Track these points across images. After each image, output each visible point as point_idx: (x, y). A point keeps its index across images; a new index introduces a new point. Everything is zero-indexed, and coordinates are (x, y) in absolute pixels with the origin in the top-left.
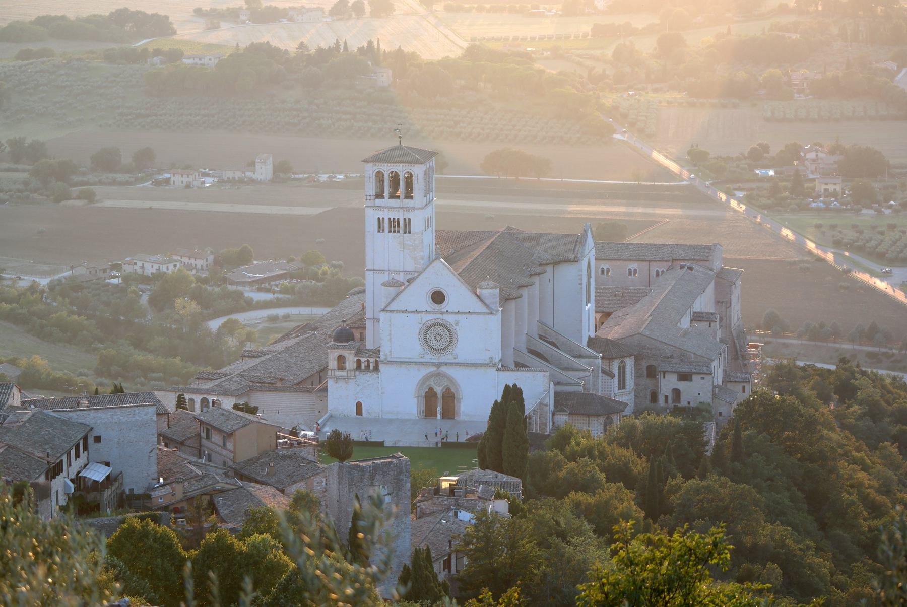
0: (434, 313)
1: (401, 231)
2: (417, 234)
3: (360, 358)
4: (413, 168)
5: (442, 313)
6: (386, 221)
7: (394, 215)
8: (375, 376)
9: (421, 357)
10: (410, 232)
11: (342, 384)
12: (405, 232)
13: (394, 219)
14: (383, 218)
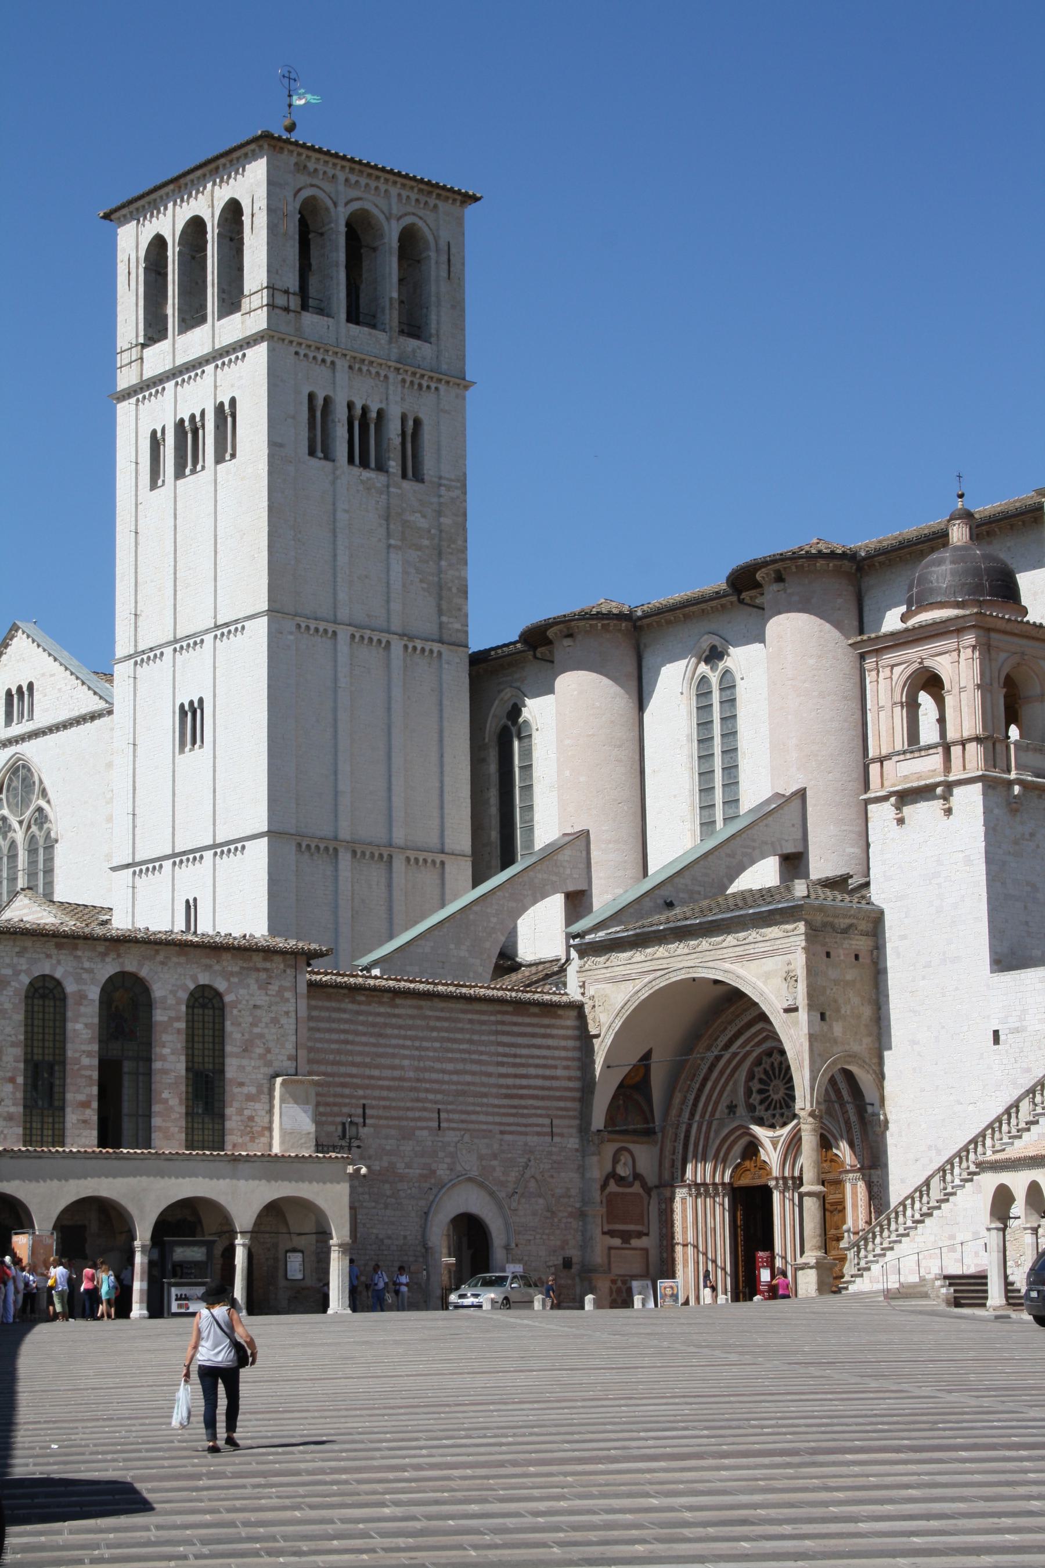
2: (449, 488)
6: (341, 414)
10: (418, 477)
12: (404, 476)
13: (365, 410)
14: (327, 400)
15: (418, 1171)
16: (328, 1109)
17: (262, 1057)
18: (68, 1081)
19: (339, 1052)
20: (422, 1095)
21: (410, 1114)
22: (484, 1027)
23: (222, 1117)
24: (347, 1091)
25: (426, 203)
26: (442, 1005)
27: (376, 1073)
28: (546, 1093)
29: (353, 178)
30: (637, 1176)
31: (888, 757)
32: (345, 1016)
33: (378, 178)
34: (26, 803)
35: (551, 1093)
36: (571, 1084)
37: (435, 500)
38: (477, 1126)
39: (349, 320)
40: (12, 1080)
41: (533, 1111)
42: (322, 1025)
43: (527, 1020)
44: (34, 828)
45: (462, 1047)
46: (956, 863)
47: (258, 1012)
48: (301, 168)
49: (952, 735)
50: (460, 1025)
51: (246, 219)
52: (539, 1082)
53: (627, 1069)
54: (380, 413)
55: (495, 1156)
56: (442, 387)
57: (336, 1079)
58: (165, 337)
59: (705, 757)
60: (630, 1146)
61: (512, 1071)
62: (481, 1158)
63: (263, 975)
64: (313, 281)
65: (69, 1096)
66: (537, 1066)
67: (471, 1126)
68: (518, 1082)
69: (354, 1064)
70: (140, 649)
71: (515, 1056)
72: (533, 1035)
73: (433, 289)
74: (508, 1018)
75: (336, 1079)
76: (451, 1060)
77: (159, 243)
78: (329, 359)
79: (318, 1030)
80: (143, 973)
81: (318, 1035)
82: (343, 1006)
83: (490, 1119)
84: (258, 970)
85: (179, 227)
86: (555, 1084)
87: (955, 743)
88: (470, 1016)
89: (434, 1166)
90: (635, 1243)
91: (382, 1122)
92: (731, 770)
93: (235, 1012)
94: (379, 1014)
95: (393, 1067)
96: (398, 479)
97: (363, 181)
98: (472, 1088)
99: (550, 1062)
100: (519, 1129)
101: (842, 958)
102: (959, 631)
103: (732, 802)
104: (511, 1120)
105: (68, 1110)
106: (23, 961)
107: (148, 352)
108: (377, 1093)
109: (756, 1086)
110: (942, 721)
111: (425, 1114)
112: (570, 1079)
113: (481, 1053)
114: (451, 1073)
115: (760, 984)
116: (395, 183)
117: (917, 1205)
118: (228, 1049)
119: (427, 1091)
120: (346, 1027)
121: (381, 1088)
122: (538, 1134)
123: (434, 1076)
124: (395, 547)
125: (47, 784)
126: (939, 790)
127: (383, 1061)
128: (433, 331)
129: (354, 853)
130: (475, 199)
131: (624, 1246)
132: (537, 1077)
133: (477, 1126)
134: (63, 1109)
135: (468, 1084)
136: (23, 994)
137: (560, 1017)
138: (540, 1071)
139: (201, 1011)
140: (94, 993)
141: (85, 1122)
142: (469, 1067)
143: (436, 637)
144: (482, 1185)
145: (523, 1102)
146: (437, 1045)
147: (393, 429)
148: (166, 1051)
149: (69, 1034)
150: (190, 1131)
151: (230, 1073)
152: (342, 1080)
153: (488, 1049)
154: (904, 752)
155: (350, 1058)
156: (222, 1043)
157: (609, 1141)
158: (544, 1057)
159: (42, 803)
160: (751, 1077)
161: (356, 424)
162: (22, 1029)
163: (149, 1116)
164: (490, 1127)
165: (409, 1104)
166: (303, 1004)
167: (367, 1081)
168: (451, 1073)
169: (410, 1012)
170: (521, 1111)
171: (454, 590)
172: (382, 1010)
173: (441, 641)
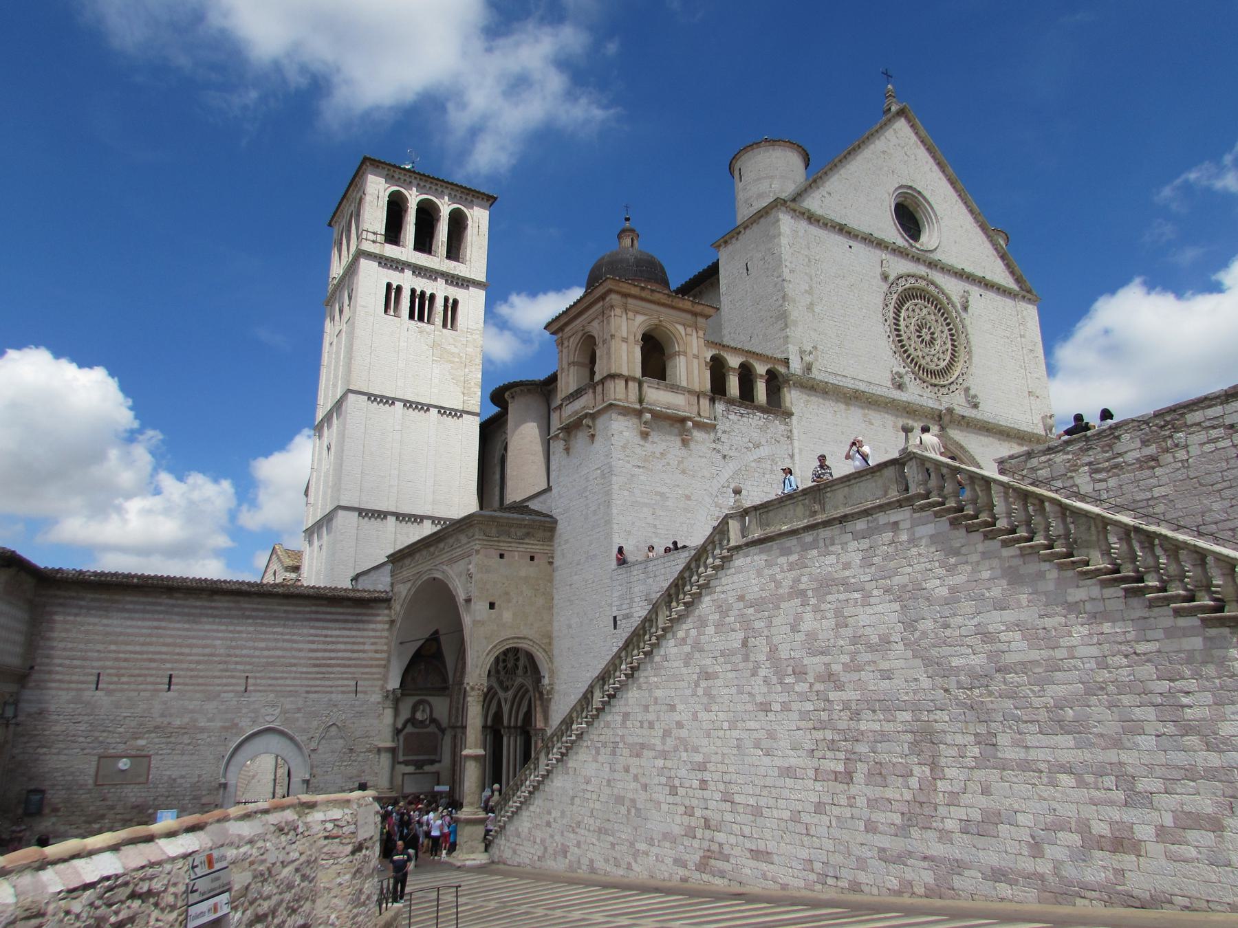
0: (917, 260)
5: (932, 265)
6: (406, 295)
8: (777, 426)
9: (900, 387)
11: (665, 444)
12: (445, 326)
13: (423, 293)
14: (399, 289)
15: (219, 724)
16: (133, 679)
19: (150, 635)
20: (233, 667)
21: (217, 681)
22: (299, 616)
24: (154, 665)
25: (466, 199)
26: (259, 600)
27: (187, 650)
28: (353, 662)
29: (422, 184)
30: (433, 721)
33: (437, 184)
35: (359, 662)
36: (378, 656)
37: (465, 339)
38: (284, 689)
39: (415, 249)
41: (340, 676)
43: (340, 610)
45: (275, 630)
46: (596, 479)
48: (390, 178)
50: (275, 614)
53: (421, 642)
54: (432, 297)
55: (299, 710)
57: (145, 656)
60: (430, 699)
61: (320, 646)
62: (284, 712)
66: (346, 643)
67: (278, 688)
68: (327, 654)
71: (326, 636)
75: (145, 656)
76: (264, 640)
82: (159, 600)
83: (297, 682)
86: (361, 655)
87: (597, 383)
88: (285, 608)
89: (235, 722)
90: (427, 768)
91: (187, 688)
94: (196, 607)
97: (428, 186)
98: (282, 660)
99: (362, 640)
100: (323, 689)
101: (517, 558)
102: (603, 297)
104: (318, 682)
108: (185, 666)
111: (233, 681)
112: (376, 652)
113: (294, 634)
114: (262, 649)
116: (447, 188)
119: (237, 663)
122: (343, 692)
123: (244, 652)
124: (436, 361)
127: (194, 641)
128: (468, 258)
131: (418, 771)
132: (345, 651)
133: (284, 689)
135: (279, 657)
137: (372, 608)
138: (349, 647)
142: (280, 644)
143: (461, 408)
145: (330, 669)
147: (439, 303)
152: (150, 656)
153: (300, 631)
155: (161, 640)
158: (353, 637)
161: (417, 300)
164: (297, 688)
168: (262, 649)
169: (226, 605)
170: (327, 676)
171: (472, 384)
172: (199, 603)
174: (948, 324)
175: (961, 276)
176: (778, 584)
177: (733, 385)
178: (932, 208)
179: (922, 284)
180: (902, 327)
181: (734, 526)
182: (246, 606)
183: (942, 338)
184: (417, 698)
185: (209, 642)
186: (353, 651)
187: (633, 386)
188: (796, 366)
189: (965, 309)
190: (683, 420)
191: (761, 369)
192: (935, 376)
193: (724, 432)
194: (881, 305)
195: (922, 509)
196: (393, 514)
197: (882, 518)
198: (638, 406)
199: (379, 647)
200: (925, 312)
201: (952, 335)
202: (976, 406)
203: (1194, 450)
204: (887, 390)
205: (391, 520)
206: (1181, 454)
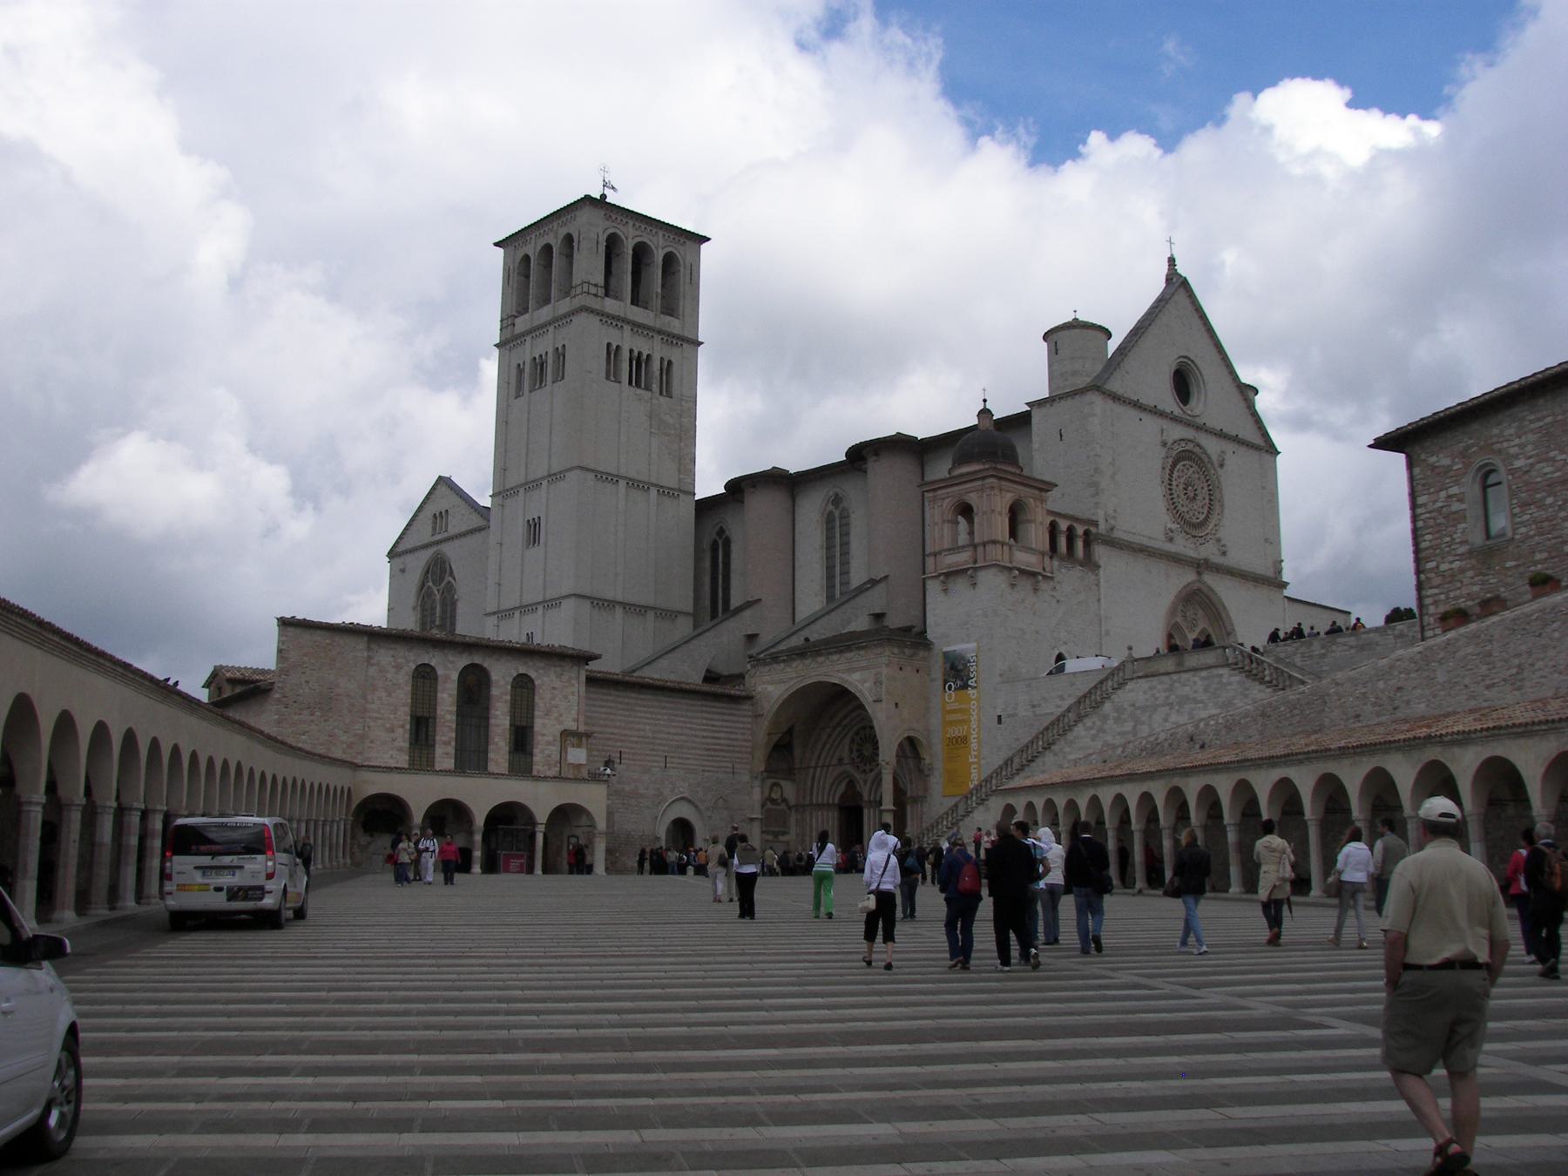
0: (1188, 424)
1: (655, 387)
2: (687, 402)
3: (1058, 520)
4: (680, 247)
6: (625, 355)
7: (642, 346)
9: (1171, 540)
10: (669, 395)
12: (661, 393)
13: (640, 353)
14: (618, 347)
15: (653, 792)
17: (556, 719)
18: (438, 729)
23: (531, 754)
24: (610, 743)
28: (731, 748)
29: (637, 225)
30: (784, 800)
31: (940, 553)
32: (611, 698)
34: (442, 579)
36: (745, 744)
39: (632, 303)
40: (403, 726)
42: (596, 703)
44: (446, 594)
47: (555, 692)
49: (977, 540)
51: (575, 244)
52: (728, 742)
56: (685, 345)
58: (526, 310)
59: (830, 558)
60: (783, 783)
61: (710, 734)
63: (558, 669)
64: (613, 281)
65: (437, 738)
69: (615, 727)
70: (507, 487)
71: (713, 726)
72: (724, 714)
73: (682, 289)
74: (708, 703)
77: (526, 258)
78: (619, 325)
79: (594, 705)
80: (485, 665)
81: (594, 709)
83: (696, 762)
84: (555, 666)
85: (539, 248)
86: (735, 743)
90: (781, 838)
92: (845, 563)
93: (541, 691)
95: (639, 730)
96: (658, 394)
102: (983, 478)
103: (845, 583)
105: (437, 746)
106: (411, 654)
107: (517, 321)
109: (855, 747)
110: (971, 533)
111: (657, 758)
112: (745, 741)
115: (859, 686)
116: (661, 228)
117: (950, 819)
118: (536, 713)
119: (660, 744)
120: (612, 705)
121: (631, 742)
122: (726, 772)
123: (663, 736)
125: (453, 567)
126: (969, 572)
128: (681, 312)
129: (625, 608)
130: (709, 239)
132: (724, 739)
134: (433, 746)
136: (411, 674)
139: (519, 690)
140: (455, 676)
141: (447, 754)
143: (677, 487)
144: (689, 801)
145: (717, 754)
146: (666, 717)
147: (656, 365)
148: (497, 713)
149: (439, 700)
150: (511, 763)
151: (536, 728)
154: (949, 550)
156: (533, 710)
157: (768, 778)
159: (450, 579)
160: (853, 741)
162: (410, 696)
163: (486, 752)
165: (648, 752)
166: (583, 688)
167: (623, 738)
172: (633, 695)
173: (681, 491)
174: (1207, 481)
175: (1220, 436)
176: (1156, 699)
177: (1062, 543)
178: (1201, 374)
179: (1190, 447)
180: (1174, 487)
181: (1129, 666)
182: (662, 698)
183: (1203, 493)
184: (774, 780)
185: (640, 726)
186: (732, 739)
187: (1006, 548)
188: (1102, 528)
189: (1222, 466)
190: (1034, 574)
191: (1080, 530)
192: (1194, 527)
193: (1058, 582)
194: (1160, 470)
195: (1234, 669)
196: (624, 605)
197: (1215, 671)
198: (1010, 565)
199: (746, 737)
200: (1187, 471)
201: (1210, 490)
202: (1224, 553)
203: (1338, 654)
204: (1161, 544)
205: (619, 611)
206: (1333, 654)
